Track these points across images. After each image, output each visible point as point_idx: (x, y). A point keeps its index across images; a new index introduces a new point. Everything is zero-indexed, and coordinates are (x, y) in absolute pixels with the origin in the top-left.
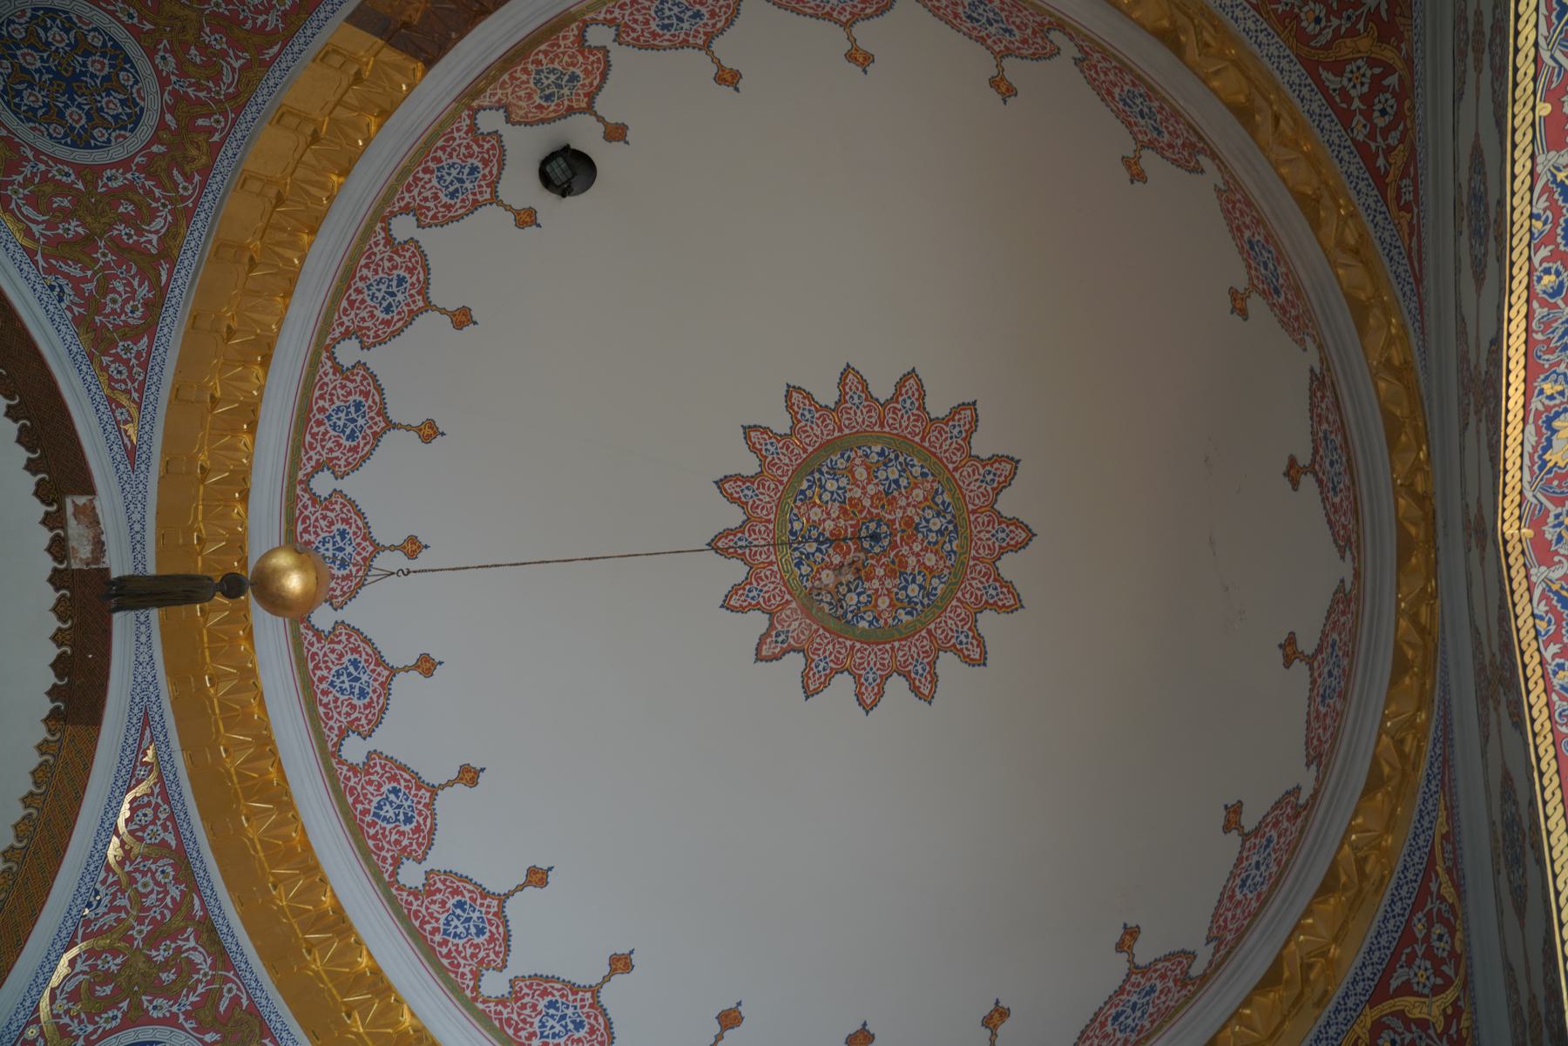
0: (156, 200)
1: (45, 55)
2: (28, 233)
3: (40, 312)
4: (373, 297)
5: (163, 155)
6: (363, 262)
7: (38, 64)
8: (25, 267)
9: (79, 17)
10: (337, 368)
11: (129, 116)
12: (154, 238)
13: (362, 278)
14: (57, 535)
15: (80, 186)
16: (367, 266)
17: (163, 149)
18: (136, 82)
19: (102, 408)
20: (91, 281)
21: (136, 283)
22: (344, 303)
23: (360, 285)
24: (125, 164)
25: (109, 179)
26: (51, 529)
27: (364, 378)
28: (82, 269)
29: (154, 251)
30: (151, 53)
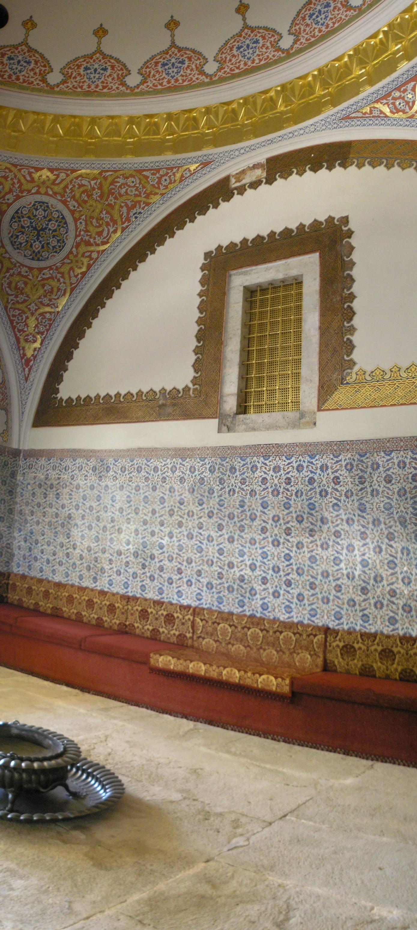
0: (74, 186)
2: (115, 231)
3: (149, 220)
4: (99, 78)
6: (79, 90)
8: (130, 230)
10: (144, 82)
12: (93, 182)
13: (89, 86)
15: (84, 217)
16: (81, 87)
21: (118, 184)
22: (105, 90)
23: (93, 87)
27: (147, 67)
28: (122, 207)
29: (99, 181)
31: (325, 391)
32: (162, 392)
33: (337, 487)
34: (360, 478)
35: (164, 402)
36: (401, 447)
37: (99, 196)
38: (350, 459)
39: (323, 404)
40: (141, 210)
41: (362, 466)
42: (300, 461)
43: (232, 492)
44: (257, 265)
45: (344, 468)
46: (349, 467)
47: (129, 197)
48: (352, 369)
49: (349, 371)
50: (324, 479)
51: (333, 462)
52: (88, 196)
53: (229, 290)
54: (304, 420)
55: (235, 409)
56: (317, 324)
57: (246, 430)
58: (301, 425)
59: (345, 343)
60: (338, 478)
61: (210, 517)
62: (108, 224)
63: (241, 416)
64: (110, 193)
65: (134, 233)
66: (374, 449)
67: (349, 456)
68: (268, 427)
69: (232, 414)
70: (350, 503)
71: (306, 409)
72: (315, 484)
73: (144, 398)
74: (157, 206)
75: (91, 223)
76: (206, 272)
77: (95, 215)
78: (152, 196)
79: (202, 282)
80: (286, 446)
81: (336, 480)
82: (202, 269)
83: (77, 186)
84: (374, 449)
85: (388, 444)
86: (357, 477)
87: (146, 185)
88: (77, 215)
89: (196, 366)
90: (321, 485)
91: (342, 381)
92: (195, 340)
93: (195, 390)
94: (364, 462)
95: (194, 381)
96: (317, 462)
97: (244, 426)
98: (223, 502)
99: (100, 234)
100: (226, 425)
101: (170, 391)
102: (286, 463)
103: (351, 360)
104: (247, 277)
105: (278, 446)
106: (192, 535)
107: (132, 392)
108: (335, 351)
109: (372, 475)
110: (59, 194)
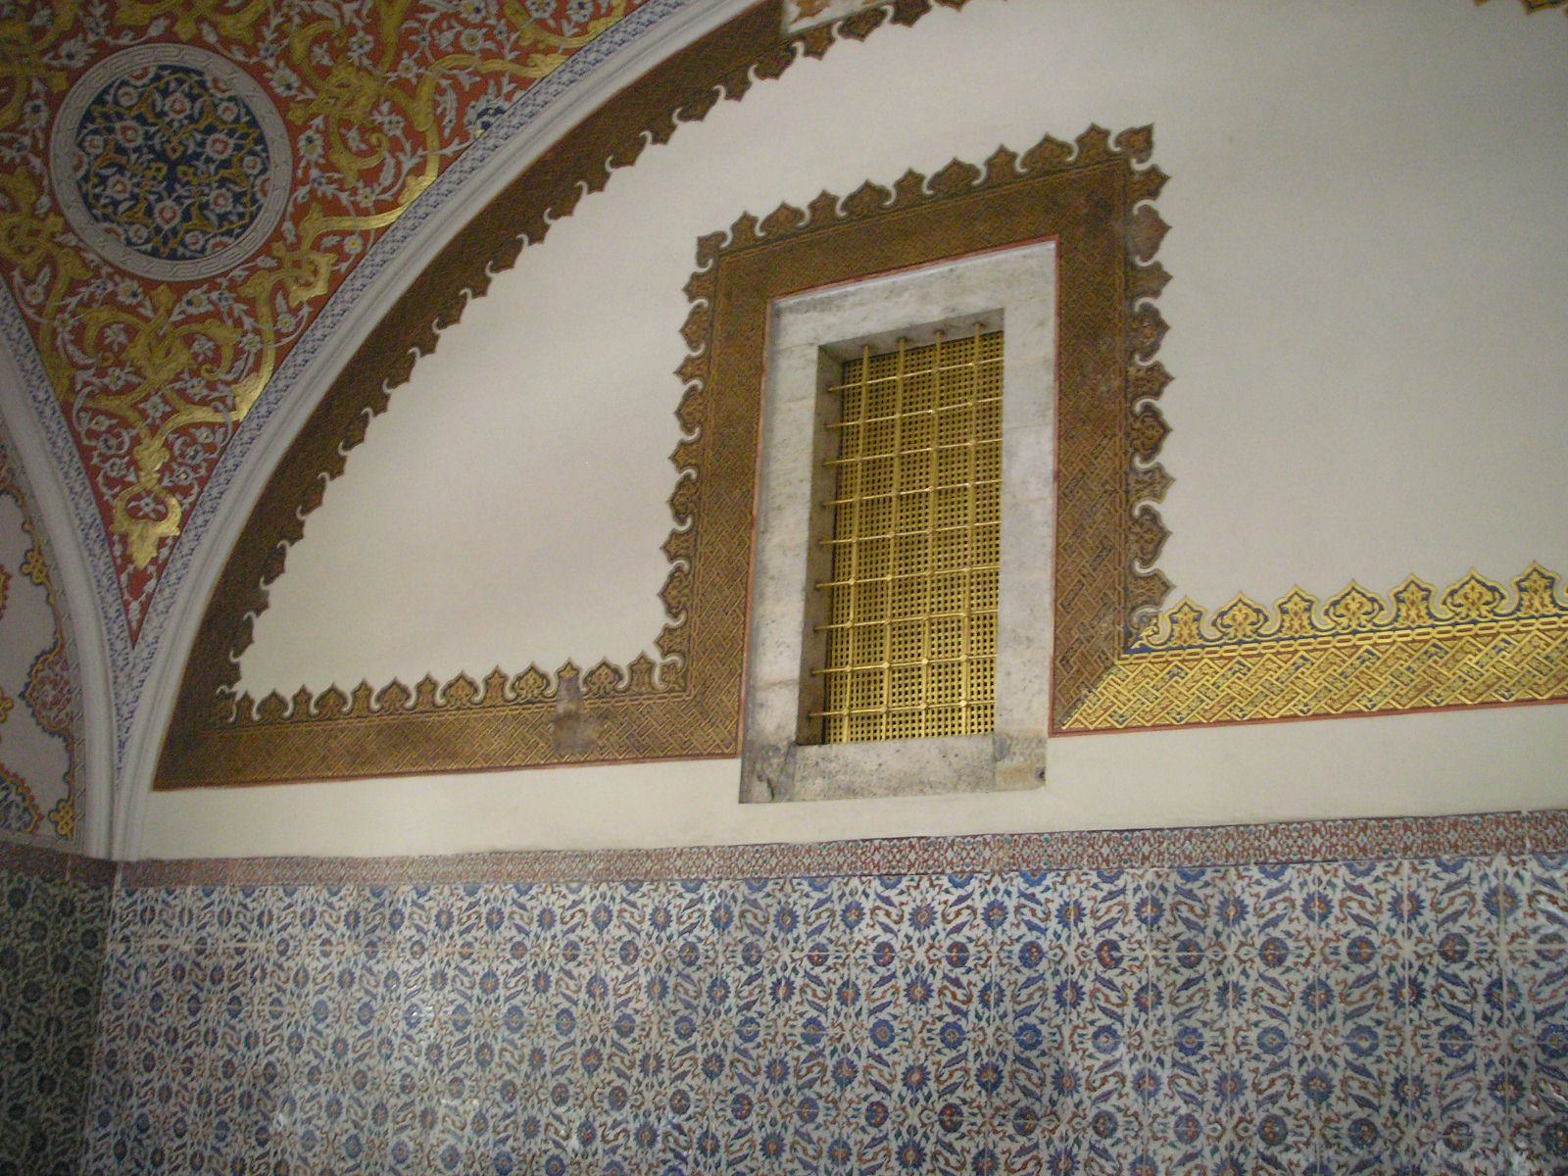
0: (288, 19)
1: (152, 198)
2: (419, 170)
5: (215, 26)
7: (169, 203)
8: (467, 166)
9: (76, 169)
11: (180, 82)
14: (841, 31)
17: (206, 28)
18: (125, 83)
19: (645, 18)
20: (454, 77)
21: (431, 17)
24: (257, 73)
25: (289, 87)
26: (831, 41)
28: (441, 91)
30: (74, 76)
31: (1075, 672)
32: (567, 675)
33: (1111, 974)
34: (1185, 946)
35: (573, 707)
36: (1316, 851)
37: (368, 55)
38: (1151, 886)
39: (1068, 714)
40: (500, 103)
41: (1191, 909)
42: (995, 890)
43: (783, 990)
44: (859, 277)
45: (1132, 915)
46: (1148, 911)
47: (464, 60)
48: (1157, 604)
49: (1150, 610)
50: (1070, 950)
51: (1100, 895)
52: (335, 54)
53: (773, 360)
54: (1008, 763)
55: (791, 729)
56: (1049, 464)
57: (827, 795)
58: (998, 779)
59: (1136, 521)
60: (1113, 946)
61: (711, 1075)
62: (396, 146)
63: (813, 751)
64: (405, 44)
65: (477, 178)
66: (1229, 855)
67: (1150, 876)
68: (894, 783)
69: (783, 745)
70: (1154, 1026)
71: (1013, 730)
72: (1043, 966)
73: (510, 695)
74: (553, 89)
75: (344, 140)
76: (703, 301)
77: (357, 114)
78: (537, 58)
79: (691, 332)
80: (951, 845)
81: (1109, 954)
82: (691, 292)
83: (297, 20)
84: (1229, 855)
85: (1273, 842)
86: (1175, 945)
87: (518, 20)
88: (297, 115)
89: (673, 596)
90: (1061, 968)
91: (1127, 642)
92: (667, 513)
93: (667, 669)
94: (1195, 898)
95: (667, 641)
96: (1048, 895)
97: (819, 781)
98: (753, 1027)
99: (370, 177)
100: (766, 778)
101: (592, 673)
102: (952, 899)
103: (1155, 575)
104: (829, 318)
105: (927, 843)
106: (655, 1135)
107: (470, 675)
108: (1103, 549)
109: (1223, 938)
110: (240, 43)
